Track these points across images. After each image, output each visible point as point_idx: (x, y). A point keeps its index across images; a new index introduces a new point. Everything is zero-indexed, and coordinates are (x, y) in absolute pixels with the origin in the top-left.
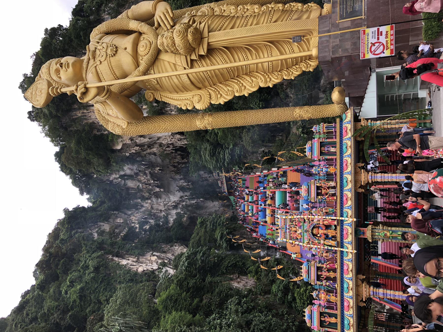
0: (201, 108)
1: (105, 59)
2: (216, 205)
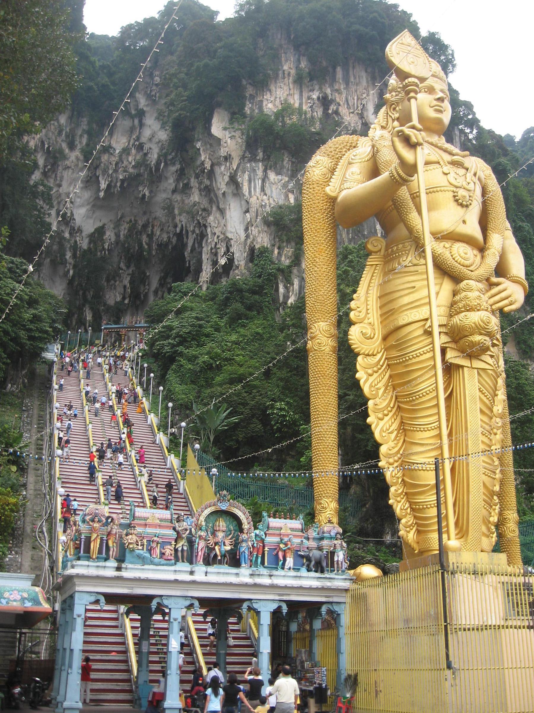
0: (351, 335)
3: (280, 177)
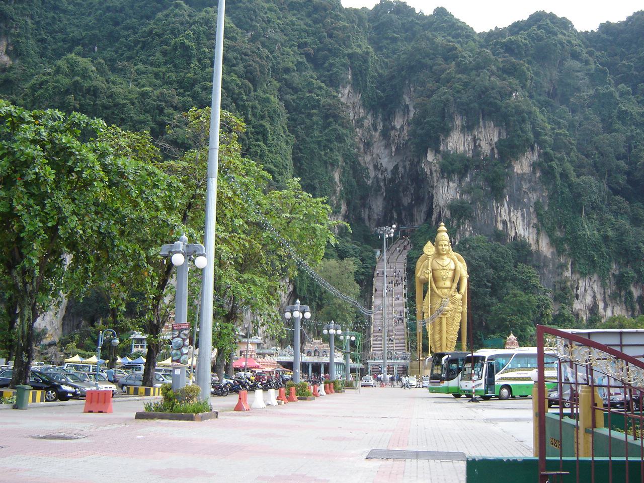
3: (454, 184)
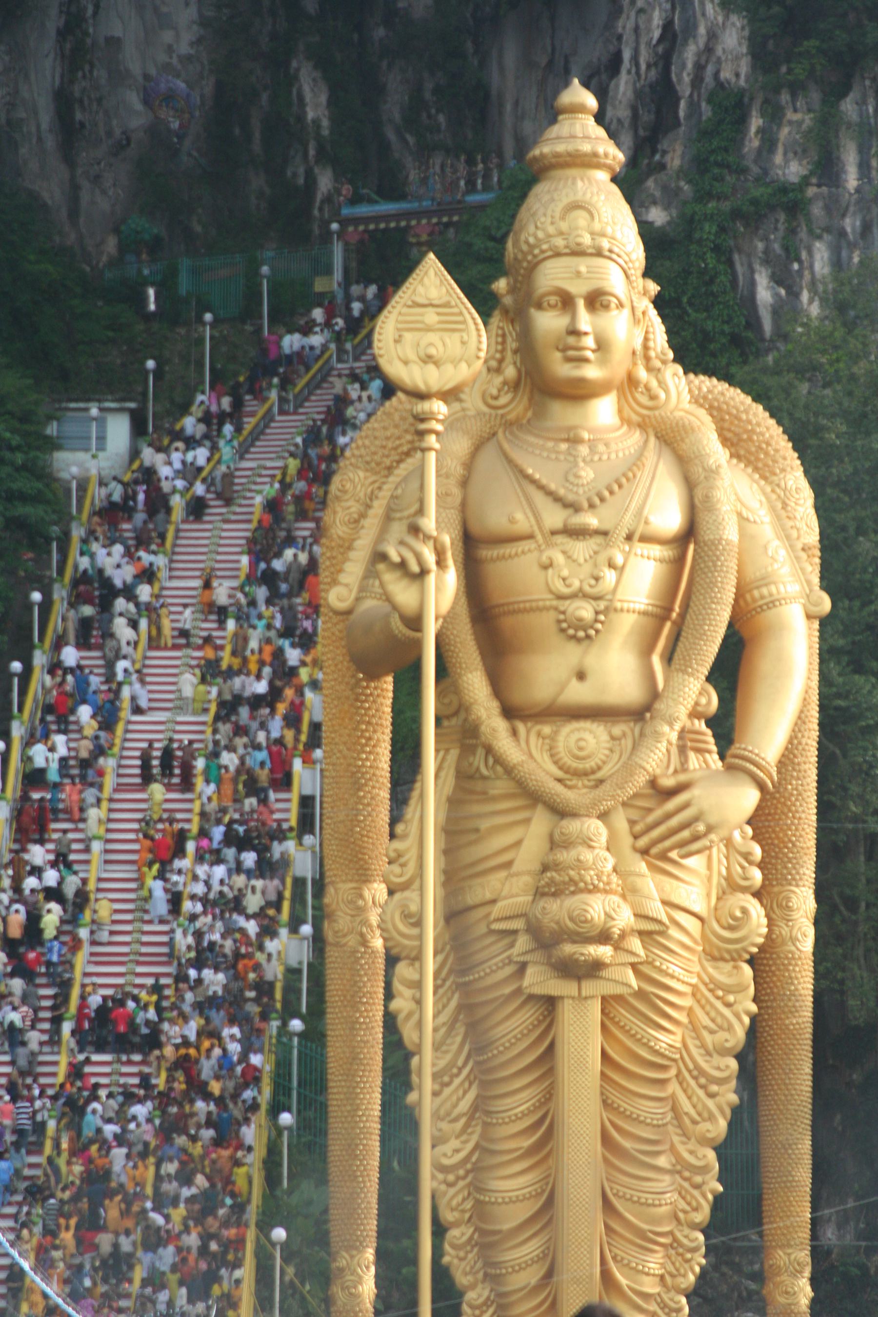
1: (551, 592)
2: (167, 36)
